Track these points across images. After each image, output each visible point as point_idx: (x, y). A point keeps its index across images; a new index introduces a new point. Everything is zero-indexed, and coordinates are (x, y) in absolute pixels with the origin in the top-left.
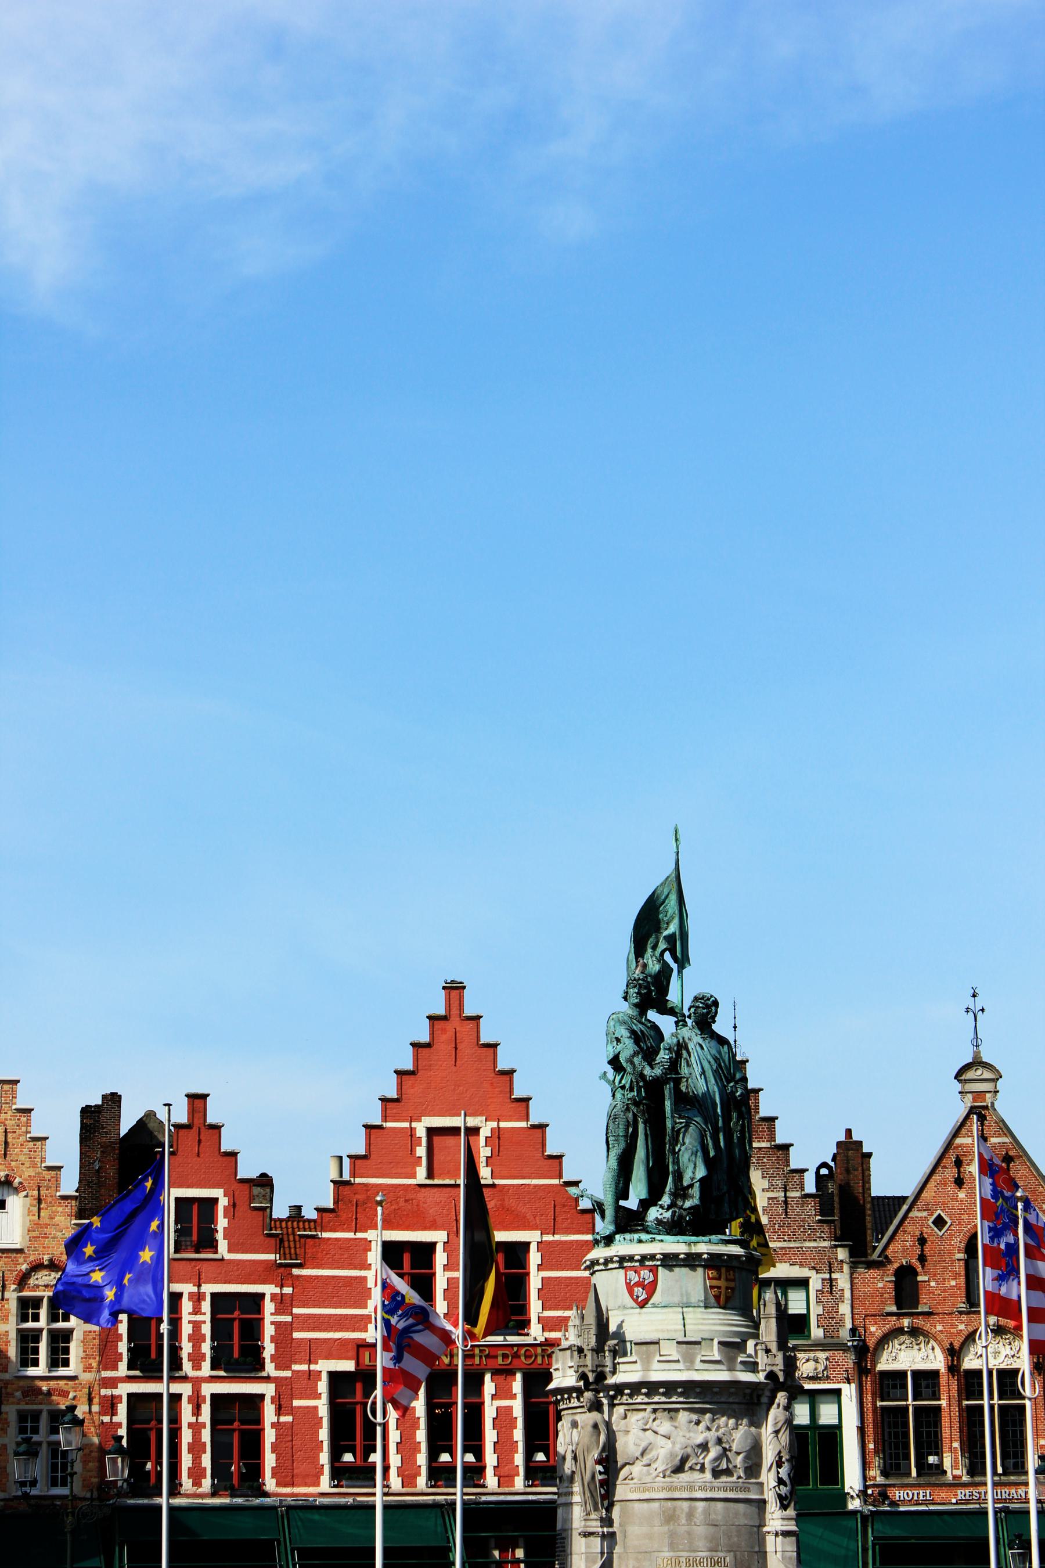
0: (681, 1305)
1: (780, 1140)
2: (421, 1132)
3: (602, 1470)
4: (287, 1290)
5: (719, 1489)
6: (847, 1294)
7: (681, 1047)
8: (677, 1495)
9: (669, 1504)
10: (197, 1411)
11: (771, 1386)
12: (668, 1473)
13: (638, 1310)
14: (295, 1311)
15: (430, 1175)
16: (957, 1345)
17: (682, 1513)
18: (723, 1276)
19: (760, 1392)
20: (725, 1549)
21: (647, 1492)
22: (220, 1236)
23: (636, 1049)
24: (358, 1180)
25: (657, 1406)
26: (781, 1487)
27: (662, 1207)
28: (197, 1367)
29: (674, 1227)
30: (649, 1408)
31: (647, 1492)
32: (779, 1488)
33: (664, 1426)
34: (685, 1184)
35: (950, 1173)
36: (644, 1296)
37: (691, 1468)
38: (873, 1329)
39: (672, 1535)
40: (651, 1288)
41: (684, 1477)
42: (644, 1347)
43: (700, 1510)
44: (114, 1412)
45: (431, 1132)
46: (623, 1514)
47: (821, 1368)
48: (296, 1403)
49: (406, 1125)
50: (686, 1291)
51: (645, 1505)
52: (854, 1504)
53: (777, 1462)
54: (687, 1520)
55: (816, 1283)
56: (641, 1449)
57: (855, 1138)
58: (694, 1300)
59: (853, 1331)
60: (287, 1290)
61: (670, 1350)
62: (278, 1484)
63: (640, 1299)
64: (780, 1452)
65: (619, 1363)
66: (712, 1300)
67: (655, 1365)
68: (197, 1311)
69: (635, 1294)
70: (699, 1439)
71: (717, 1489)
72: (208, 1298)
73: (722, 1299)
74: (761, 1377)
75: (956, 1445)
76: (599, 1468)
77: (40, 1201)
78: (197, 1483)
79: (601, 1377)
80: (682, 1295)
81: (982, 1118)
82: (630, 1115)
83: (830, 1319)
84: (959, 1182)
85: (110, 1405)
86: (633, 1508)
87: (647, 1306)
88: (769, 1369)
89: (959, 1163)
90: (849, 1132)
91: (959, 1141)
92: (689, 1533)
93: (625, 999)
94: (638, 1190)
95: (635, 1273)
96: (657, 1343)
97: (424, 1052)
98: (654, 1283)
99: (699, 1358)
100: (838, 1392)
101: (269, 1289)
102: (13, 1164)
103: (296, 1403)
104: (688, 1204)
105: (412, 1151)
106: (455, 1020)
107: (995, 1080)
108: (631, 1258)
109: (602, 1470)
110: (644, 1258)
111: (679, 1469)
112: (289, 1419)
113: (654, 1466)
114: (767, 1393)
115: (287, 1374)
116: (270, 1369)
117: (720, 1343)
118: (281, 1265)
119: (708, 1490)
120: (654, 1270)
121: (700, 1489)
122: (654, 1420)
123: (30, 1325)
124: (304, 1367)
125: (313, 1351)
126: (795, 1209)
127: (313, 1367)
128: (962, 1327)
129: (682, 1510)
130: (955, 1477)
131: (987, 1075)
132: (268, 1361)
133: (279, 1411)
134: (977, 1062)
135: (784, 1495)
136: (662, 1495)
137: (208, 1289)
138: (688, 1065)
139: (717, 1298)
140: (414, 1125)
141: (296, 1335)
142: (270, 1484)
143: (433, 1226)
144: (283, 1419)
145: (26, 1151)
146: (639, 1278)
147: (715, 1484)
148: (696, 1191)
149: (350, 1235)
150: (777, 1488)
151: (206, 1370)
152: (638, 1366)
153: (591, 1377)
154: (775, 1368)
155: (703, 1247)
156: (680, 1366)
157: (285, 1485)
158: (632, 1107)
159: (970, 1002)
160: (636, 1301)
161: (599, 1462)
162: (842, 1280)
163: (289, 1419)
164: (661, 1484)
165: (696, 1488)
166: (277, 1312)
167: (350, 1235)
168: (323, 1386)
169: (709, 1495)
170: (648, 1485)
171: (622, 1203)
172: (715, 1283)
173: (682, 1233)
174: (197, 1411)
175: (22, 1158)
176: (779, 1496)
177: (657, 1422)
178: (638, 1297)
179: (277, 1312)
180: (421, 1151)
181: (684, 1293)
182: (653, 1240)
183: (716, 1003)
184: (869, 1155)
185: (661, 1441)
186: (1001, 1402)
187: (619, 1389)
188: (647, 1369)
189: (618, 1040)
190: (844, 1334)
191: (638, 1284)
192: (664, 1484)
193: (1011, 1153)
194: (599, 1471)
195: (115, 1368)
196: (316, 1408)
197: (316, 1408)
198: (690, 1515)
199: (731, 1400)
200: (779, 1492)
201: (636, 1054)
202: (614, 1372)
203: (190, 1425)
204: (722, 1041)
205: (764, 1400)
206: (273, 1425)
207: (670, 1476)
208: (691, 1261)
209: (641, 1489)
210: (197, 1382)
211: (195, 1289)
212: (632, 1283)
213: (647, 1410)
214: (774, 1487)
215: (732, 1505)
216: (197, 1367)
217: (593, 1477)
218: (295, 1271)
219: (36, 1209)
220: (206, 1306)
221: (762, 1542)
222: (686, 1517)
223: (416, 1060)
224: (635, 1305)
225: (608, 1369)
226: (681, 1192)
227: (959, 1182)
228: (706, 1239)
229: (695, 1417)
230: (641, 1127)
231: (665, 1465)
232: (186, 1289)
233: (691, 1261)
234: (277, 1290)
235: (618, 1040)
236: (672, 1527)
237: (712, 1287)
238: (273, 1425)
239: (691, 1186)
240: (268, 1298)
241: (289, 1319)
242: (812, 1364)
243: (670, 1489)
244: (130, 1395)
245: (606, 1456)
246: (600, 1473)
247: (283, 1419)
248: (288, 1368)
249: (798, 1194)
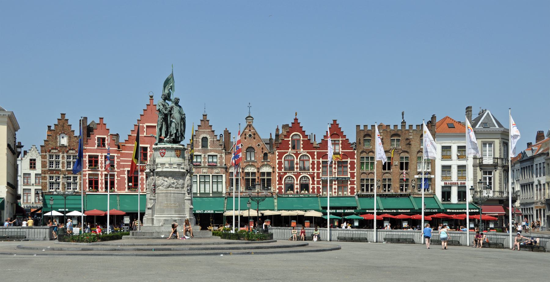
1: (213, 130)
2: (145, 126)
4: (119, 155)
5: (176, 191)
6: (224, 158)
7: (172, 108)
8: (168, 192)
10: (102, 177)
11: (187, 172)
13: (162, 158)
14: (121, 159)
15: (146, 134)
16: (244, 168)
22: (106, 145)
23: (163, 107)
24: (133, 135)
27: (167, 138)
28: (102, 168)
29: (170, 142)
33: (166, 179)
34: (172, 134)
35: (244, 136)
38: (229, 164)
39: (167, 199)
40: (164, 153)
41: (170, 189)
42: (162, 165)
44: (85, 177)
45: (147, 126)
46: (158, 195)
47: (219, 171)
48: (121, 176)
49: (142, 125)
52: (223, 195)
55: (219, 156)
56: (161, 183)
57: (227, 130)
58: (172, 156)
59: (225, 165)
60: (119, 155)
61: (167, 166)
62: (118, 190)
65: (157, 168)
66: (176, 156)
67: (164, 168)
68: (102, 158)
70: (172, 182)
72: (104, 156)
73: (178, 156)
74: (185, 171)
75: (243, 185)
76: (153, 187)
78: (102, 190)
79: (154, 170)
81: (250, 127)
82: (162, 121)
83: (221, 162)
84: (245, 138)
85: (85, 175)
88: (186, 169)
89: (245, 135)
90: (226, 129)
91: (245, 131)
92: (170, 199)
93: (162, 98)
94: (163, 135)
96: (165, 164)
97: (146, 111)
98: (165, 153)
99: (173, 167)
100: (222, 175)
101: (115, 155)
103: (121, 176)
104: (172, 138)
105: (143, 130)
106: (151, 105)
107: (253, 120)
108: (161, 148)
110: (163, 147)
111: (168, 187)
112: (120, 178)
114: (186, 174)
115: (119, 170)
116: (116, 169)
117: (177, 164)
118: (118, 150)
120: (165, 150)
121: (172, 191)
123: (69, 160)
124: (122, 169)
125: (124, 166)
126: (215, 142)
127: (124, 169)
128: (245, 164)
130: (242, 191)
131: (251, 119)
132: (115, 168)
133: (118, 177)
134: (249, 117)
136: (165, 192)
137: (104, 154)
138: (173, 111)
139: (177, 156)
140: (144, 125)
141: (121, 163)
142: (116, 190)
143: (147, 144)
144: (118, 178)
148: (174, 135)
149: (131, 145)
151: (103, 169)
152: (161, 168)
153: (152, 170)
154: (188, 169)
155: (175, 146)
156: (169, 168)
157: (119, 190)
158: (162, 119)
159: (249, 105)
160: (161, 156)
161: (153, 186)
162: (223, 155)
163: (120, 178)
166: (117, 159)
167: (131, 145)
168: (126, 173)
169: (174, 192)
171: (160, 137)
172: (177, 153)
173: (171, 143)
174: (102, 177)
176: (188, 192)
179: (117, 159)
180: (145, 130)
182: (165, 144)
183: (179, 99)
184: (230, 133)
185: (165, 182)
186: (252, 178)
187: (157, 172)
188: (163, 168)
189: (160, 106)
190: (223, 165)
191: (162, 153)
193: (255, 133)
195: (86, 168)
196: (125, 177)
197: (125, 177)
198: (170, 196)
201: (163, 108)
202: (156, 169)
203: (100, 179)
204: (180, 107)
205: (186, 175)
206: (116, 180)
208: (172, 149)
210: (102, 172)
211: (101, 154)
215: (178, 194)
216: (102, 168)
217: (152, 188)
218: (121, 152)
220: (103, 157)
221: (184, 201)
223: (144, 113)
224: (161, 156)
225: (155, 169)
226: (171, 135)
227: (245, 138)
228: (175, 144)
229: (172, 178)
230: (164, 123)
232: (99, 154)
233: (172, 149)
234: (117, 155)
235: (160, 106)
237: (176, 154)
238: (116, 180)
239: (173, 134)
240: (115, 156)
241: (119, 160)
242: (217, 170)
243: (167, 191)
244: (89, 174)
247: (118, 178)
248: (119, 169)
249: (216, 140)
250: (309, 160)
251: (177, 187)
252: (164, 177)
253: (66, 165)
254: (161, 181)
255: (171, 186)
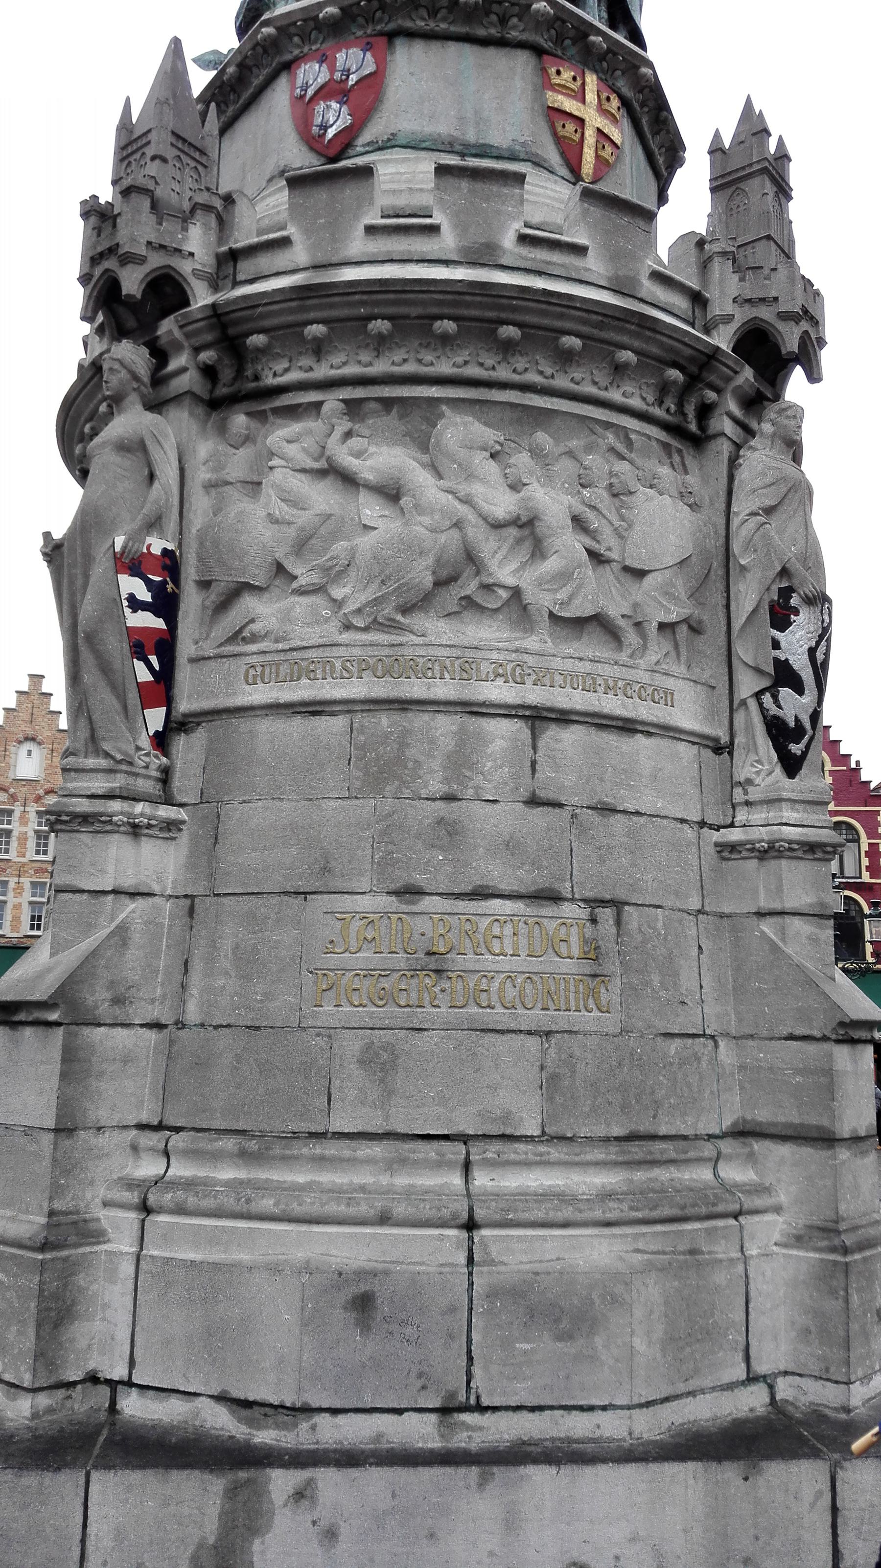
0: (458, 148)
3: (145, 595)
5: (571, 680)
8: (415, 689)
9: (384, 720)
12: (388, 610)
17: (430, 755)
18: (591, 96)
19: (711, 396)
20: (589, 894)
21: (305, 681)
25: (359, 393)
26: (785, 692)
30: (332, 401)
31: (305, 681)
32: (775, 697)
36: (345, 120)
37: (469, 603)
43: (498, 746)
50: (476, 112)
51: (297, 725)
53: (772, 608)
54: (446, 780)
63: (331, 133)
64: (784, 572)
69: (318, 120)
71: (559, 679)
77: (52, 751)
80: (461, 119)
86: (252, 734)
87: (351, 152)
95: (321, 62)
102: (37, 727)
109: (145, 595)
113: (338, 592)
119: (529, 681)
122: (348, 435)
129: (432, 741)
135: (792, 724)
145: (46, 720)
146: (332, 69)
147: (557, 663)
150: (767, 699)
154: (766, 313)
164: (357, 652)
165: (485, 667)
169: (534, 695)
170: (312, 654)
175: (43, 724)
177: (355, 443)
178: (325, 127)
181: (470, 115)
191: (325, 92)
192: (370, 651)
194: (132, 598)
199: (615, 396)
200: (774, 710)
207: (391, 626)
209: (284, 669)
212: (310, 92)
213: (325, 408)
214: (758, 695)
219: (49, 756)
222: (445, 768)
225: (186, 267)
229: (490, 435)
231: (374, 587)
236: (388, 805)
245: (165, 551)
246: (135, 604)
250: (857, 841)
251: (581, 608)
252: (353, 408)
253: (31, 844)
254: (300, 485)
255: (470, 587)
